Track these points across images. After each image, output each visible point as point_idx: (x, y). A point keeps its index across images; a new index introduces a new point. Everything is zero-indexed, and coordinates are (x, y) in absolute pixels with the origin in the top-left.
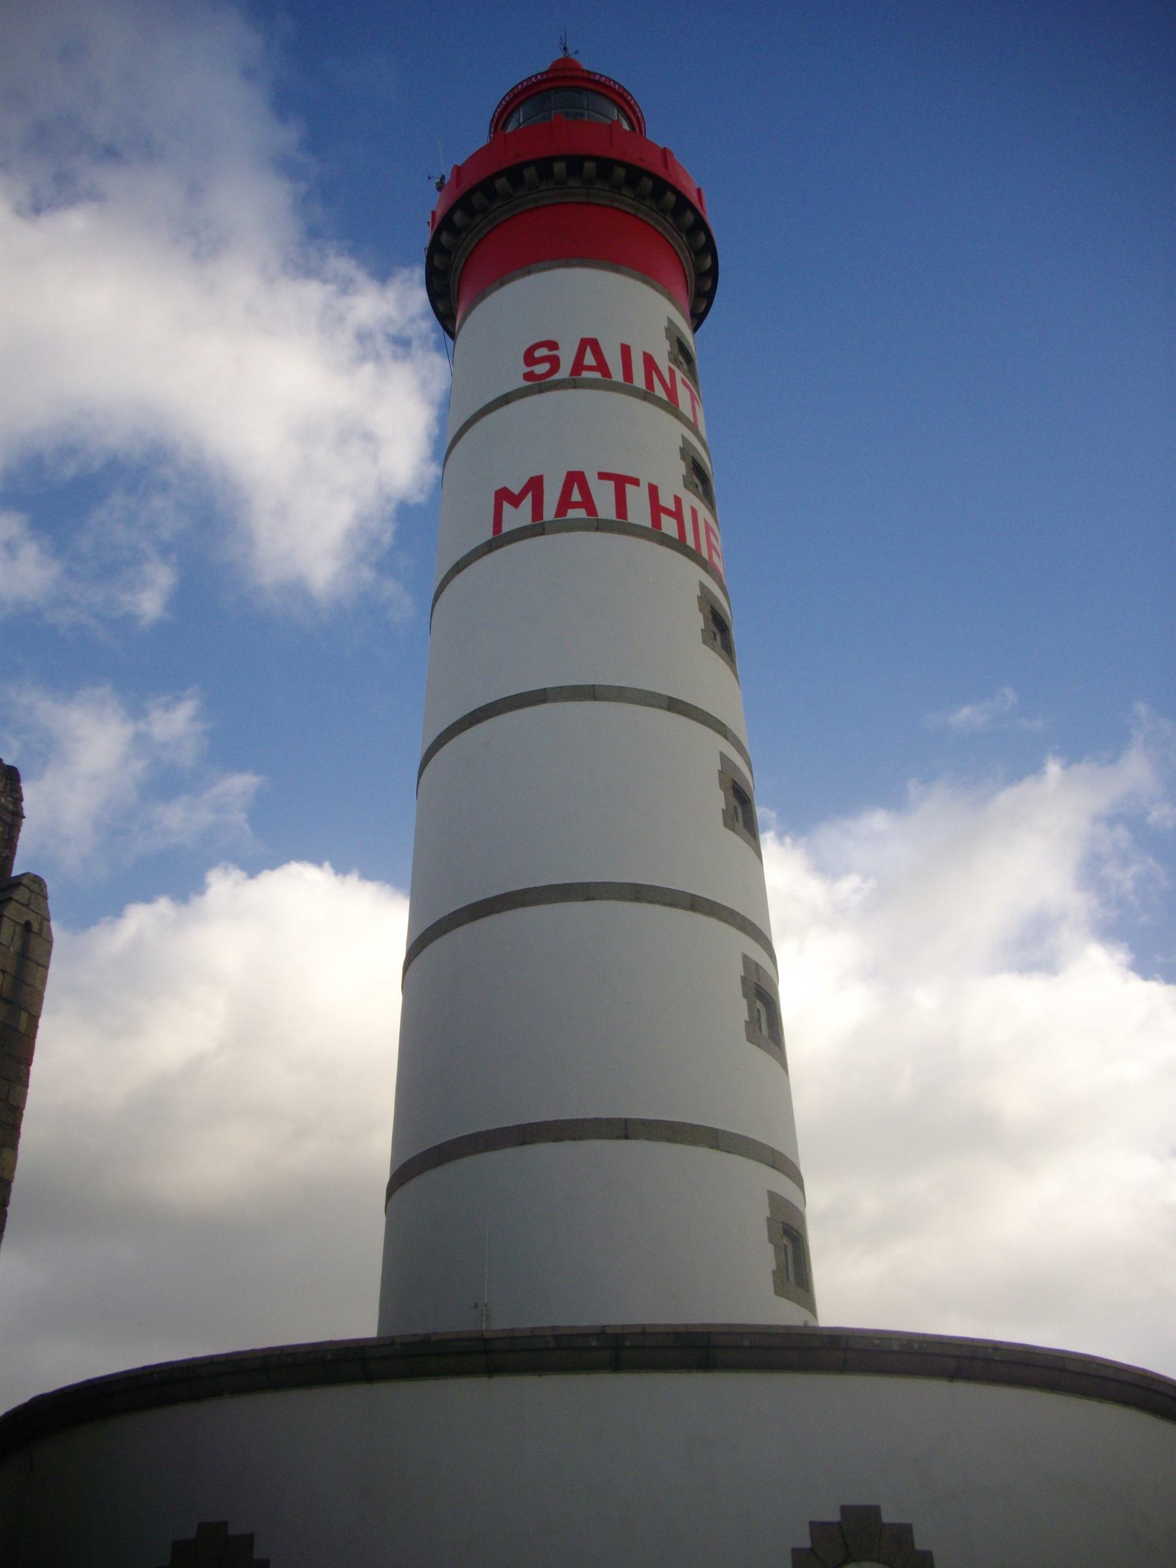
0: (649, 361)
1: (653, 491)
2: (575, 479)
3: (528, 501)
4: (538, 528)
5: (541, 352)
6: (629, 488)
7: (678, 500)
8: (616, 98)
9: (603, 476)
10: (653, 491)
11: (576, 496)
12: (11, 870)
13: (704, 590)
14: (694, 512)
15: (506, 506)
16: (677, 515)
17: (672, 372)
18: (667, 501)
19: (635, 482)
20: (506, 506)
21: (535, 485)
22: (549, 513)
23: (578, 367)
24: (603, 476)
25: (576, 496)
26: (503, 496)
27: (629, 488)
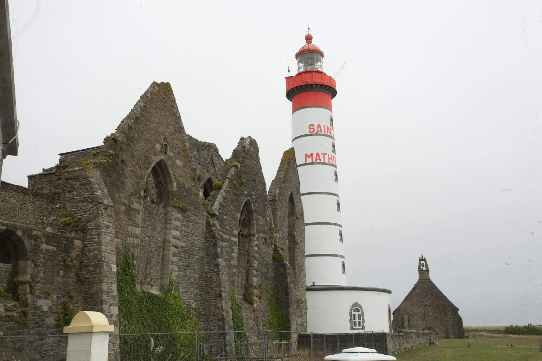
0: (327, 127)
1: (328, 155)
3: (311, 157)
5: (311, 127)
6: (325, 155)
8: (320, 54)
9: (322, 154)
10: (328, 155)
11: (318, 158)
14: (333, 156)
15: (307, 158)
16: (331, 159)
17: (331, 128)
18: (330, 157)
20: (307, 158)
21: (312, 154)
22: (314, 161)
23: (318, 131)
24: (322, 154)
25: (318, 158)
26: (306, 155)
27: (325, 155)
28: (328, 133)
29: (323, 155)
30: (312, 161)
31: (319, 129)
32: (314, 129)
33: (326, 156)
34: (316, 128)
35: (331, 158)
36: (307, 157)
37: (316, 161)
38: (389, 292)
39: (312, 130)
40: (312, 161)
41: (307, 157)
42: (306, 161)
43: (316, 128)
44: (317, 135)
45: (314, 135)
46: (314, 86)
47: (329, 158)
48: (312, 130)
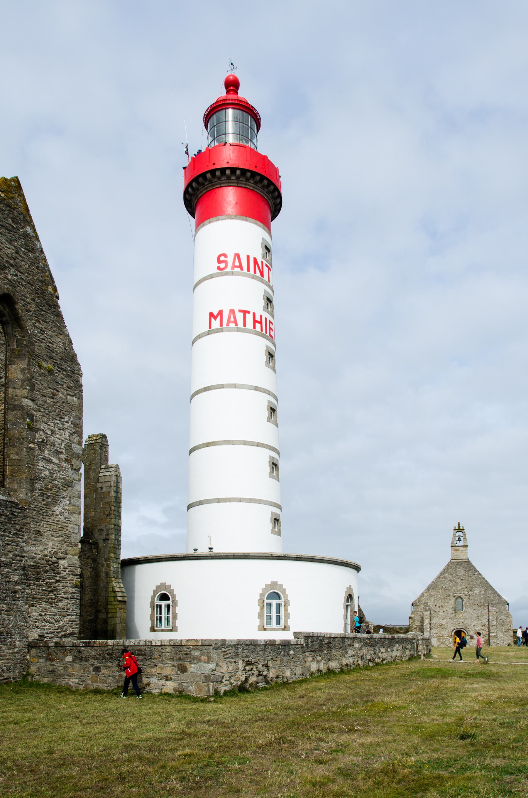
2: (232, 311)
3: (219, 318)
4: (221, 330)
5: (222, 258)
6: (247, 314)
7: (261, 317)
9: (240, 311)
10: (254, 314)
11: (232, 319)
12: (118, 545)
13: (267, 346)
15: (212, 319)
16: (261, 323)
18: (258, 318)
19: (249, 312)
20: (212, 319)
21: (220, 313)
23: (234, 266)
24: (240, 311)
25: (232, 319)
27: (247, 314)
28: (255, 272)
29: (242, 314)
30: (221, 325)
31: (237, 264)
32: (225, 262)
33: (249, 317)
34: (230, 260)
35: (259, 320)
36: (212, 318)
37: (228, 325)
38: (357, 568)
39: (222, 265)
40: (221, 325)
41: (212, 319)
42: (210, 327)
43: (230, 260)
44: (232, 274)
45: (227, 274)
46: (228, 172)
47: (255, 321)
48: (222, 265)
